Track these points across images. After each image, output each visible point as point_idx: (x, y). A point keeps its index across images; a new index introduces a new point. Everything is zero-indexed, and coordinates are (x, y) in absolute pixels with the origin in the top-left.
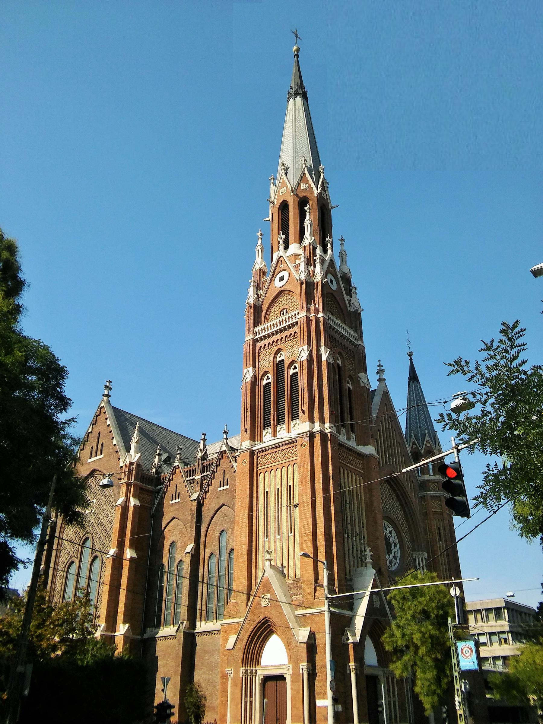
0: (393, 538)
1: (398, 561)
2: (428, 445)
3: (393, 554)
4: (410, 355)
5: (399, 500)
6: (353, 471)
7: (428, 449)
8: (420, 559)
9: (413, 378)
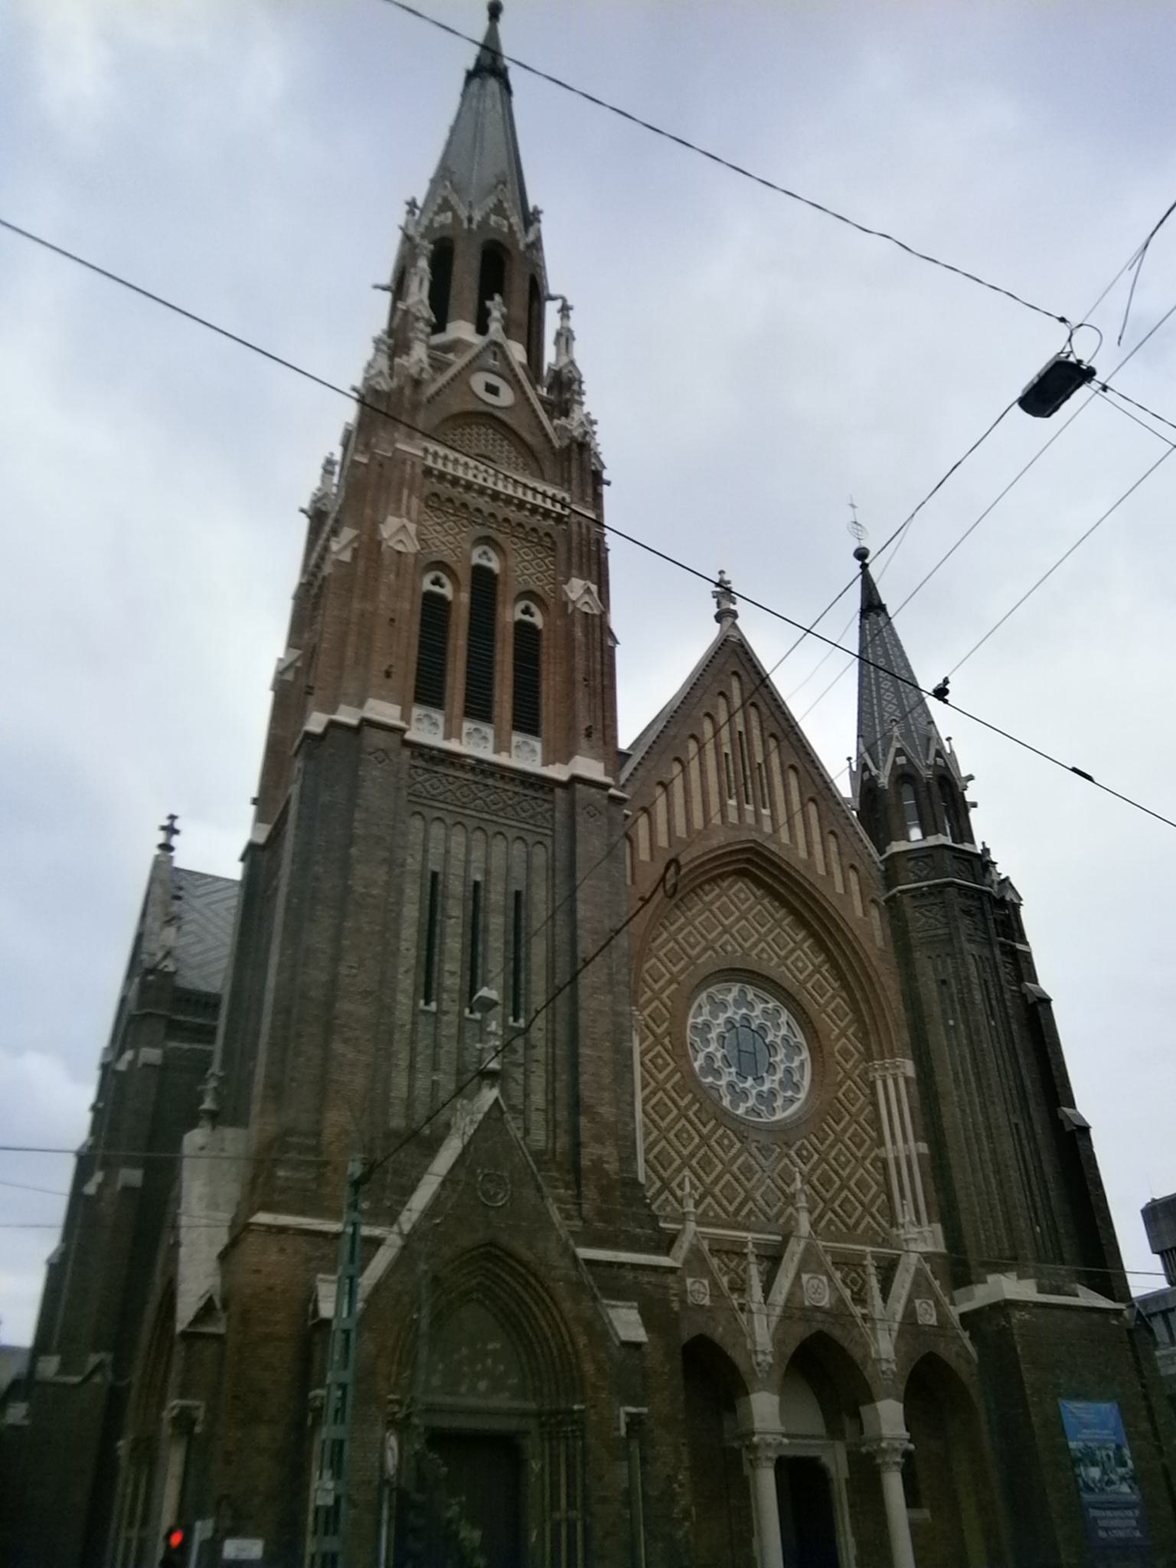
0: (784, 1031)
1: (802, 1095)
2: (902, 760)
3: (779, 1075)
4: (861, 555)
5: (801, 922)
6: (491, 829)
7: (900, 771)
8: (890, 1082)
9: (872, 606)
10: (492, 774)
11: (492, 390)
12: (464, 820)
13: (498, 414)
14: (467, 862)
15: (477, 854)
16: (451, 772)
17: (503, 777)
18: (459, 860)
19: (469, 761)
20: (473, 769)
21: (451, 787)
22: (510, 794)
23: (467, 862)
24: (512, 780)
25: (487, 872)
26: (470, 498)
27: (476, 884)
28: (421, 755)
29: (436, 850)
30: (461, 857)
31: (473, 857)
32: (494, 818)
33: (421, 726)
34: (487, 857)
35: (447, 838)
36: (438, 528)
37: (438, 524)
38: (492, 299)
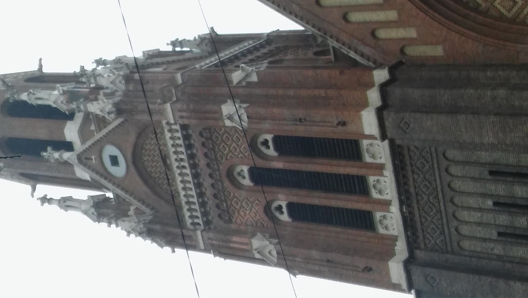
10: (407, 191)
11: (114, 161)
12: (443, 168)
13: (129, 155)
14: (480, 210)
15: (472, 202)
16: (417, 218)
17: (405, 184)
18: (482, 216)
19: (404, 210)
20: (409, 206)
21: (429, 219)
22: (416, 176)
23: (480, 210)
24: (404, 176)
25: (484, 195)
26: (209, 192)
27: (495, 204)
28: (415, 242)
29: (481, 232)
30: (479, 215)
31: (475, 206)
32: (439, 189)
33: (389, 225)
34: (469, 194)
35: (467, 223)
36: (242, 213)
37: (238, 213)
38: (46, 151)
